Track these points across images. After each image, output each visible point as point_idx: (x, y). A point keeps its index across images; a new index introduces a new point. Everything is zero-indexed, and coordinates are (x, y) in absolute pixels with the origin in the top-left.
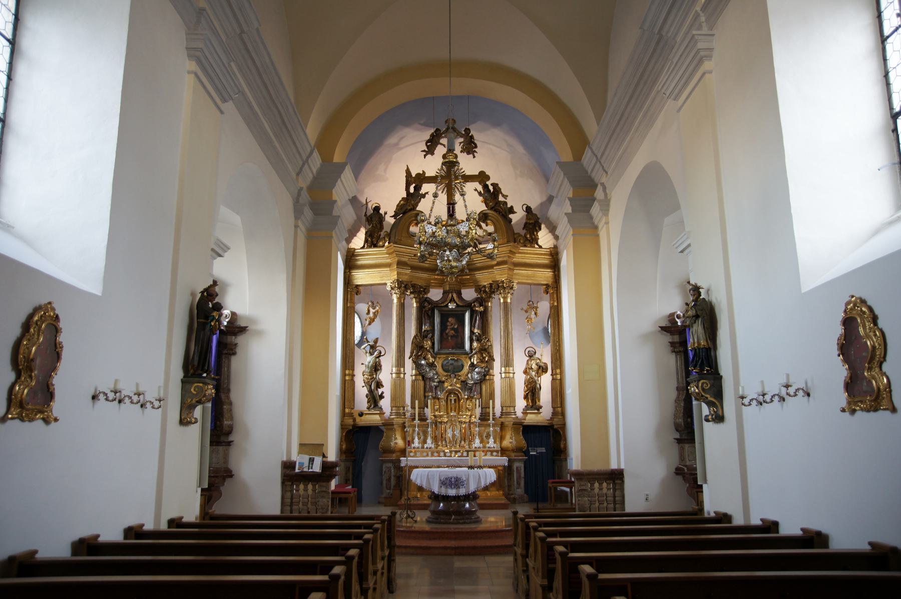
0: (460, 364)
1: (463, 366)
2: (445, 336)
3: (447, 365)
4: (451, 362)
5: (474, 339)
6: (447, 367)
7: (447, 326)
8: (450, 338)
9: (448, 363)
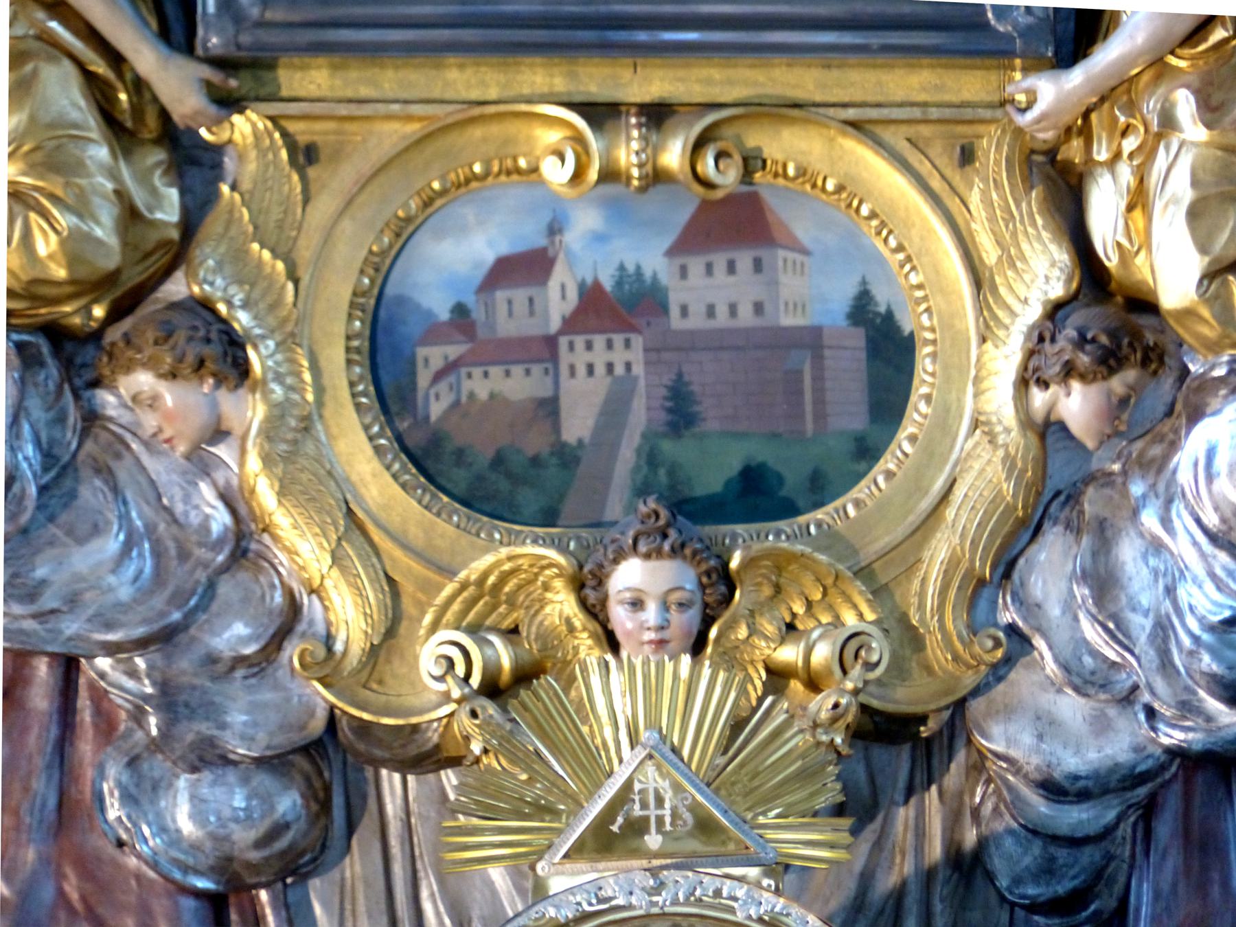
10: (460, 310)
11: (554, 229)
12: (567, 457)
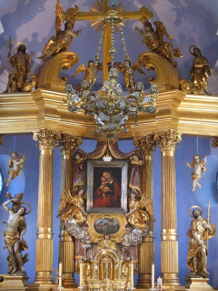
0: (115, 223)
1: (118, 226)
2: (99, 193)
3: (101, 224)
4: (105, 222)
5: (132, 196)
6: (101, 228)
7: (102, 181)
8: (104, 195)
9: (101, 222)
10: (98, 224)
11: (103, 221)
12: (103, 231)
